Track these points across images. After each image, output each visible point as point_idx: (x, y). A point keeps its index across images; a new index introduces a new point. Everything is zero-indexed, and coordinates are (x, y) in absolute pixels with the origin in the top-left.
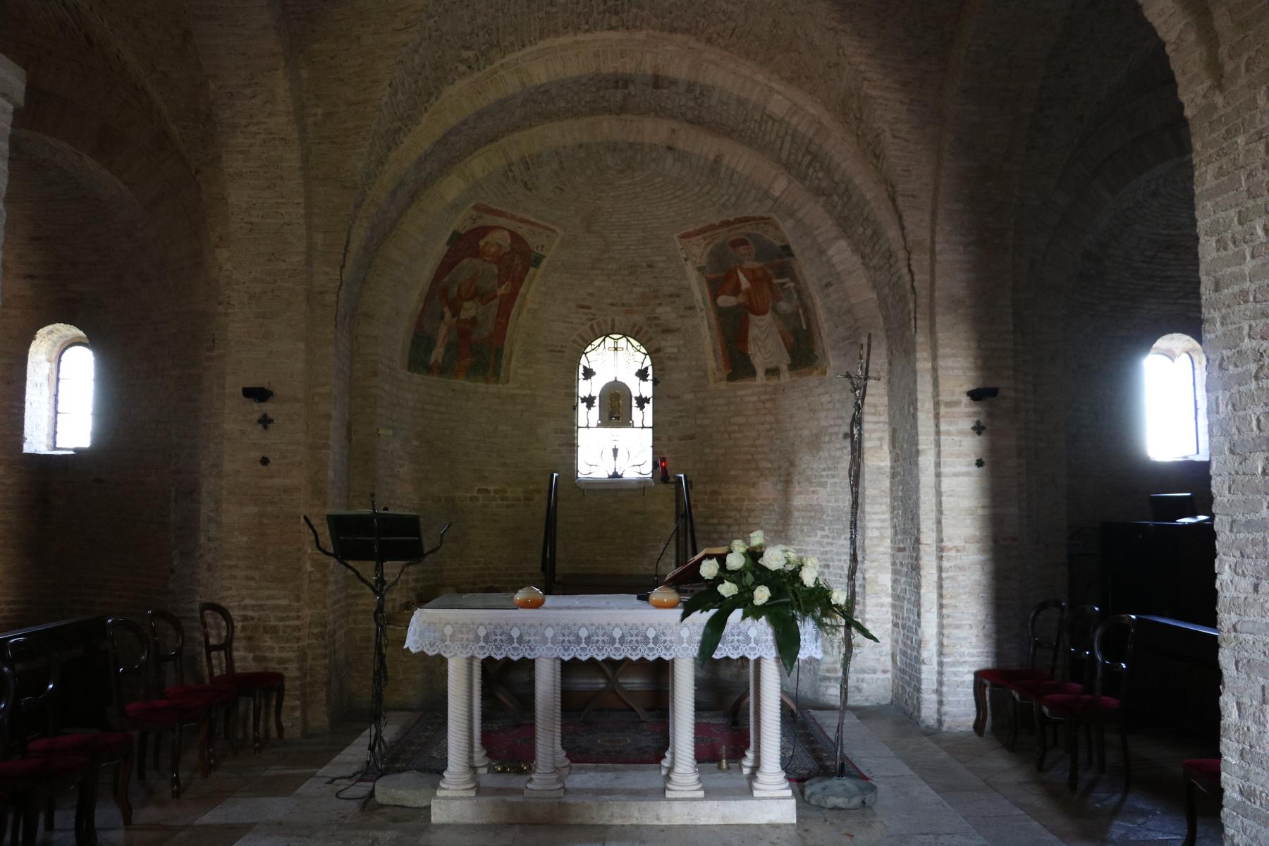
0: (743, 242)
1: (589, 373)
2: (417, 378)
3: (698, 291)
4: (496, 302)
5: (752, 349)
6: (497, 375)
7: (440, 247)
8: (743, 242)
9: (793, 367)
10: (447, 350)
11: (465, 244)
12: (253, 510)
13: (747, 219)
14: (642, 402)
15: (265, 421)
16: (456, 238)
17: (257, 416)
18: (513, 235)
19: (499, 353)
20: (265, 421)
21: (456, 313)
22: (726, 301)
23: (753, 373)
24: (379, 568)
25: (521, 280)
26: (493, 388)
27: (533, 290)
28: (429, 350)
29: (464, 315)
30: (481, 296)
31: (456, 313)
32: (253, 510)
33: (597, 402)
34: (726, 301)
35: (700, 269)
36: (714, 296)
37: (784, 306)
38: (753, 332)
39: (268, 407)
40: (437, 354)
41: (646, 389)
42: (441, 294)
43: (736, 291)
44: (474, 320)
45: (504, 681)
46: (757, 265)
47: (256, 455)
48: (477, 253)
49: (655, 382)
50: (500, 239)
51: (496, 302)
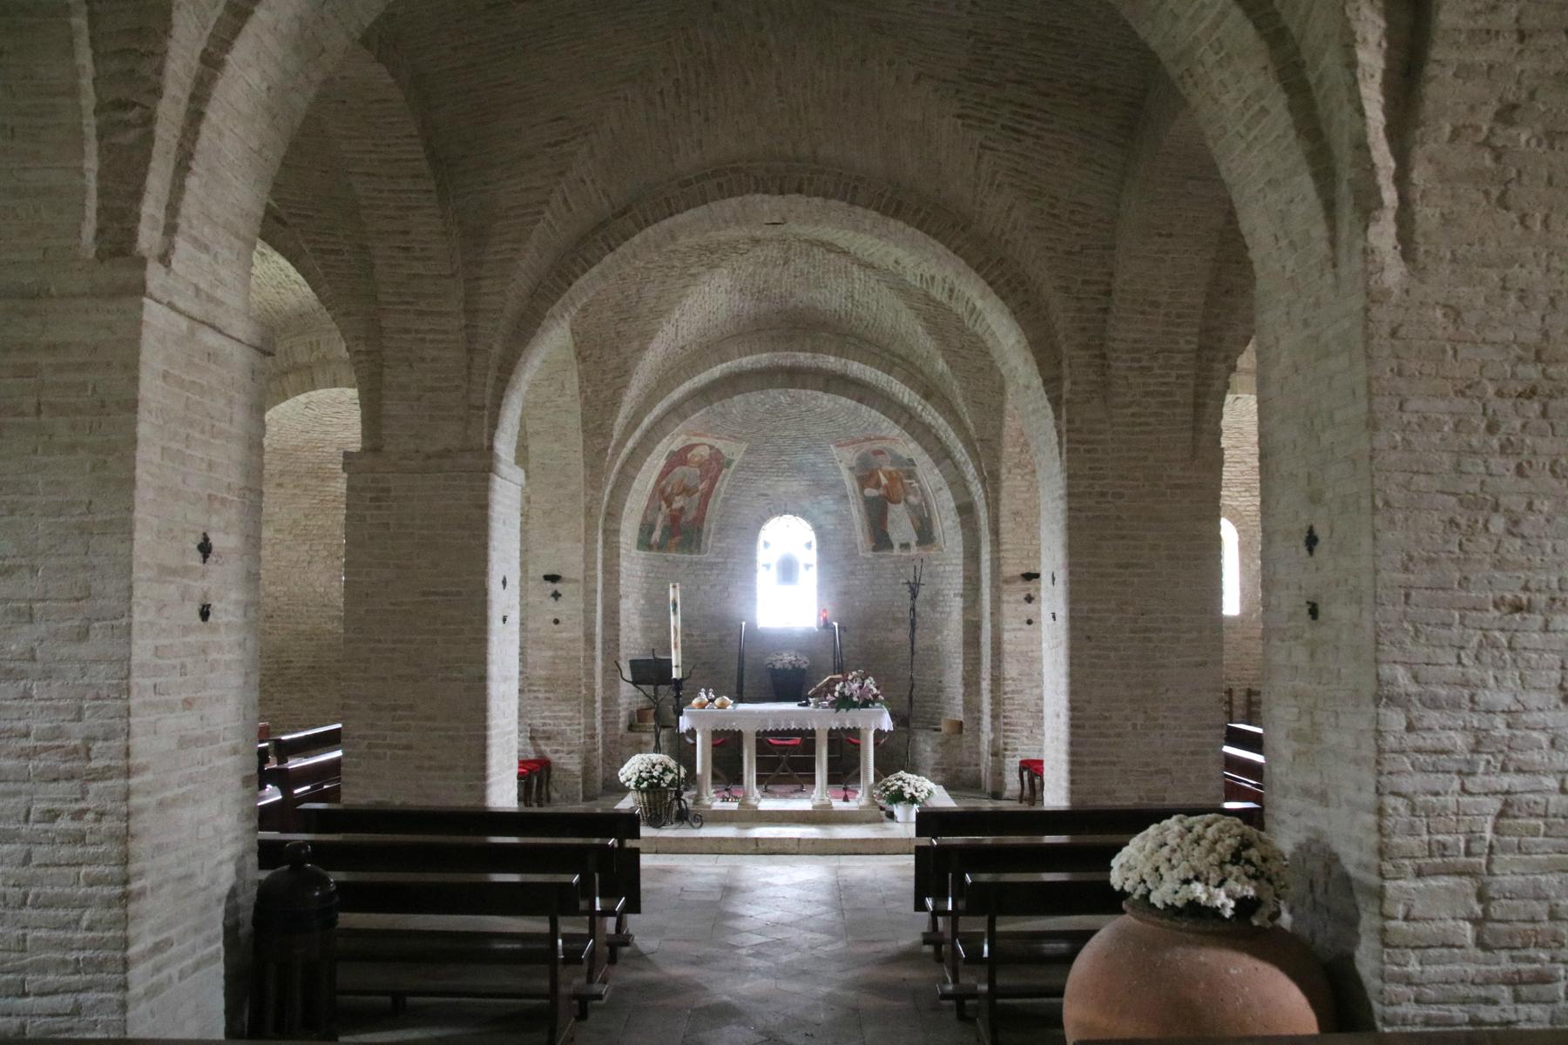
0: (882, 453)
1: (766, 545)
2: (642, 554)
3: (849, 481)
4: (697, 495)
5: (890, 529)
6: (698, 547)
7: (663, 462)
8: (882, 453)
9: (919, 543)
10: (663, 532)
11: (678, 458)
12: (550, 653)
13: (883, 438)
14: (807, 567)
15: (556, 595)
16: (672, 454)
17: (550, 592)
18: (711, 447)
19: (700, 530)
20: (556, 595)
21: (669, 505)
22: (870, 492)
23: (891, 546)
24: (656, 690)
25: (716, 477)
26: (695, 557)
27: (722, 486)
28: (651, 533)
29: (676, 505)
30: (687, 491)
31: (669, 505)
32: (550, 653)
33: (774, 568)
34: (870, 492)
35: (851, 469)
36: (862, 488)
37: (912, 499)
38: (891, 516)
39: (558, 586)
40: (656, 535)
41: (812, 556)
42: (661, 494)
43: (878, 485)
44: (682, 509)
45: (727, 747)
46: (891, 469)
47: (553, 617)
48: (684, 462)
49: (819, 551)
50: (704, 452)
51: (697, 495)
